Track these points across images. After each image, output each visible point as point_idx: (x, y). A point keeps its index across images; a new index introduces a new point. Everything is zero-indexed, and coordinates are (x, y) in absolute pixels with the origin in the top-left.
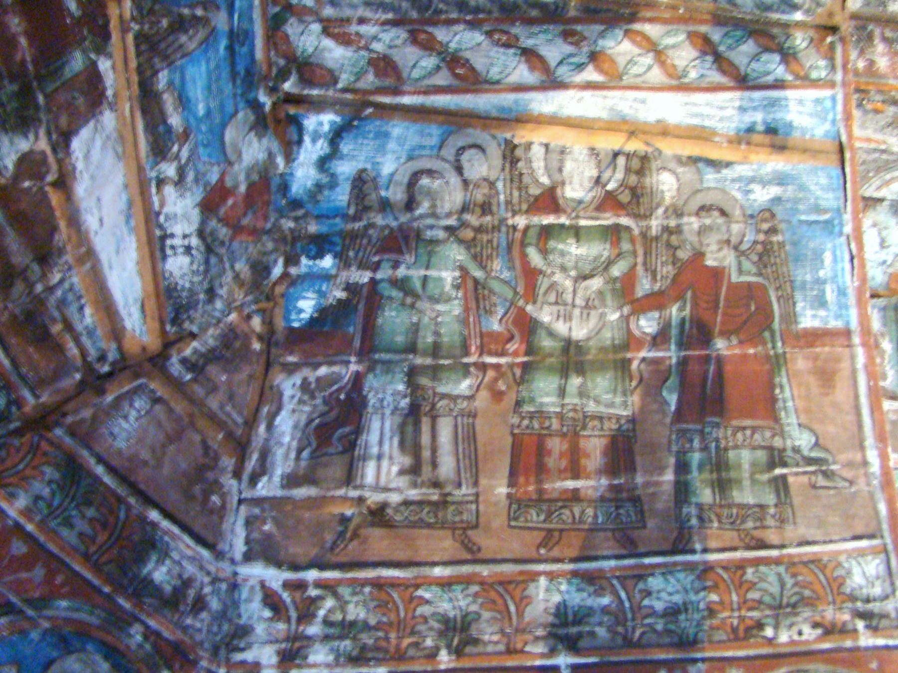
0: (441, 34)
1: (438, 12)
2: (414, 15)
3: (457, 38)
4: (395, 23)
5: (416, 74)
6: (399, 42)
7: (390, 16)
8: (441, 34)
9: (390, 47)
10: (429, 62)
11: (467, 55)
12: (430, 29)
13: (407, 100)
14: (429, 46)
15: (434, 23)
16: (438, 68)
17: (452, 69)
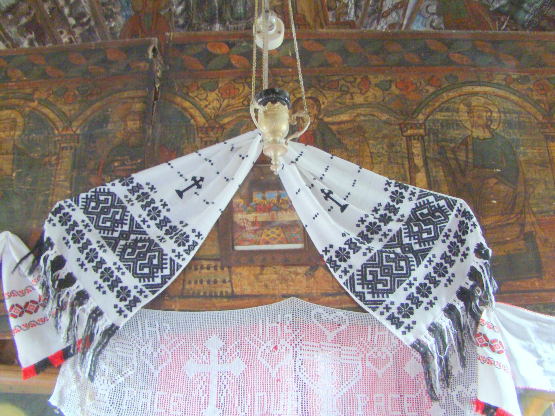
0: (385, 9)
1: (377, 8)
2: (376, 15)
3: (388, 5)
4: (378, 22)
5: (397, 19)
6: (385, 21)
7: (376, 22)
8: (385, 9)
9: (386, 24)
10: (394, 14)
11: (394, 3)
12: (383, 12)
13: (405, 22)
14: (388, 13)
15: (381, 11)
16: (397, 12)
17: (398, 9)
